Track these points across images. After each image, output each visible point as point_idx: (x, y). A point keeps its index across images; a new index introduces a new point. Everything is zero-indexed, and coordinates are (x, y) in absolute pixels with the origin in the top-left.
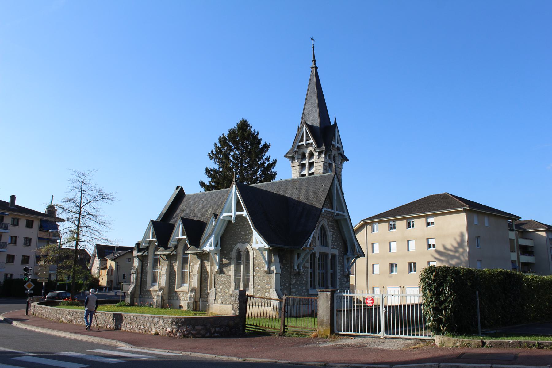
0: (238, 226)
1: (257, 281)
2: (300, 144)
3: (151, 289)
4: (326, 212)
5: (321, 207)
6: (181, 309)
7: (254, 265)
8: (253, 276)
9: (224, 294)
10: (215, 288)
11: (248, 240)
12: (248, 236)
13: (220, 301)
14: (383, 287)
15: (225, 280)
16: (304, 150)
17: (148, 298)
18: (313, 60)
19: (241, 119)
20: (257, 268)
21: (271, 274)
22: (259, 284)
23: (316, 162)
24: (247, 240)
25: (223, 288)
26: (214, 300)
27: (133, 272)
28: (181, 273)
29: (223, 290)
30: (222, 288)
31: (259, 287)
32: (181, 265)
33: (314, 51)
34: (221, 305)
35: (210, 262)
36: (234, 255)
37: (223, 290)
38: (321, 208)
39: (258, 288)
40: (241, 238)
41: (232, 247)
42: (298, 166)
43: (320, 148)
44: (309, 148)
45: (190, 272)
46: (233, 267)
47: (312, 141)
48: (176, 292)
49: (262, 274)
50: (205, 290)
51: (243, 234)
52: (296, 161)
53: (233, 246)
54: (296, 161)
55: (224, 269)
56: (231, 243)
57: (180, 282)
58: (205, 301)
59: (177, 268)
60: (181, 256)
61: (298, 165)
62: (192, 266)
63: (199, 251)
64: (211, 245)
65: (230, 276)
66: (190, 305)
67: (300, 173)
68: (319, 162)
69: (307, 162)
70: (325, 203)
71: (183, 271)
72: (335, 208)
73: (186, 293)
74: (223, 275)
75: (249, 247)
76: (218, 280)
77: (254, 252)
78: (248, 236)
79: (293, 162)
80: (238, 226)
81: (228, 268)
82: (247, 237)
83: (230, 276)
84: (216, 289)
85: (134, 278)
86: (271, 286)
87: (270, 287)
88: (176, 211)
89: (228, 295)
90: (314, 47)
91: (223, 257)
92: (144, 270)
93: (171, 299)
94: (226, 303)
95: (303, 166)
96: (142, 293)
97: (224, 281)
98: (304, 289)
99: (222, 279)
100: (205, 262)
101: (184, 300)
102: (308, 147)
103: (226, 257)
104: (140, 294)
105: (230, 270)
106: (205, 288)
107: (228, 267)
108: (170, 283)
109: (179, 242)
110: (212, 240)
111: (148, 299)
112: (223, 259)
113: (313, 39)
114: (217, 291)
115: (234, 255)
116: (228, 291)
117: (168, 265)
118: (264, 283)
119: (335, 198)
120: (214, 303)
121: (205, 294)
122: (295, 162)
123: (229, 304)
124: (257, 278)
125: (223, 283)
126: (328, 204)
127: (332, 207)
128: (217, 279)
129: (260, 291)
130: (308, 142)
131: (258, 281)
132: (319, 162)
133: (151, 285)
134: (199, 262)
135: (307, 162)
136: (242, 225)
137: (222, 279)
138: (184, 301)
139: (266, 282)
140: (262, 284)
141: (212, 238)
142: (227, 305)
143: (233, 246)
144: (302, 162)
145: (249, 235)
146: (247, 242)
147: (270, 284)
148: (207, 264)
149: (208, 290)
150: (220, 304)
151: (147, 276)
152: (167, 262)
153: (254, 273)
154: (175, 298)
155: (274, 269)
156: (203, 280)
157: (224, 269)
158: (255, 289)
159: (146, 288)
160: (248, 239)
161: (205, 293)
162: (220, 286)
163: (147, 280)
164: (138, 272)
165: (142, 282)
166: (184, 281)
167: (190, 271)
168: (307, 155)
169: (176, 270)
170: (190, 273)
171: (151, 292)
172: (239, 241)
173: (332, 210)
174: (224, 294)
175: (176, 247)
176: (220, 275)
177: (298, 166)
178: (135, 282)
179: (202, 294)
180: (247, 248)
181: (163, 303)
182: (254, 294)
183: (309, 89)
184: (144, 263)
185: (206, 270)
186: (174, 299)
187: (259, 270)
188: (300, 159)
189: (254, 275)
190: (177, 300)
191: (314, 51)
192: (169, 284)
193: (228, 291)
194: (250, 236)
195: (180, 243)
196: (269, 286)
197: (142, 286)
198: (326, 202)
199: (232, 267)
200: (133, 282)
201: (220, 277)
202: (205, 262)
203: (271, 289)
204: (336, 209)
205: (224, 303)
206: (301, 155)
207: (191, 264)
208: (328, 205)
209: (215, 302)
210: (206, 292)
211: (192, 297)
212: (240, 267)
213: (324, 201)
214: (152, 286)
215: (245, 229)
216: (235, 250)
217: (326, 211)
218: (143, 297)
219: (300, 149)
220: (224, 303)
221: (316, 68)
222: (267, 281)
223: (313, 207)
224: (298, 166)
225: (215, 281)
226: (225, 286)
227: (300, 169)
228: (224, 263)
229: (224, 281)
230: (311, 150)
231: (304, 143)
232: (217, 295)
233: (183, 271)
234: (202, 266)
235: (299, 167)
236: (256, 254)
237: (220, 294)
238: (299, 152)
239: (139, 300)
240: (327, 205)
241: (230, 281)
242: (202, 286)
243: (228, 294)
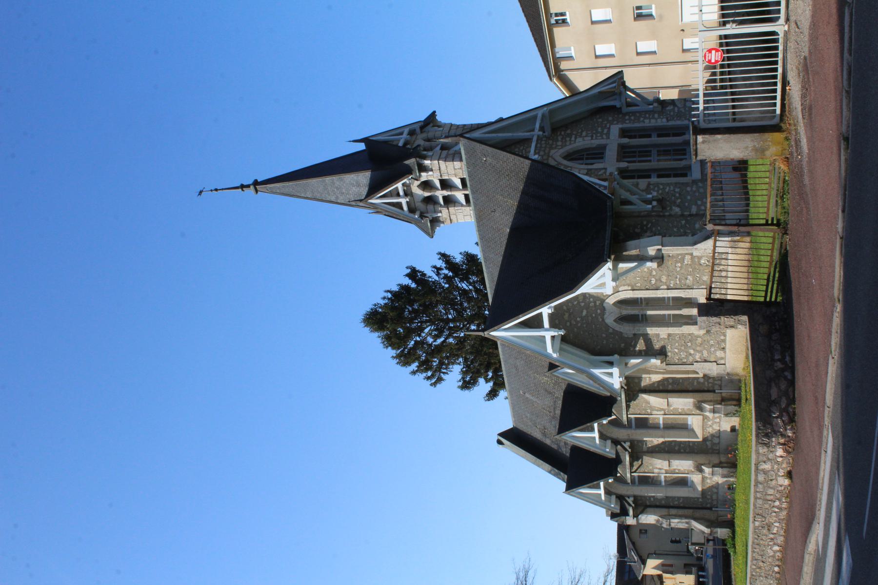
0: (571, 323)
1: (678, 282)
2: (405, 208)
3: (700, 489)
4: (537, 151)
5: (528, 162)
6: (737, 428)
7: (647, 289)
8: (668, 289)
9: (706, 346)
10: (695, 364)
11: (598, 303)
12: (591, 302)
13: (720, 354)
14: (682, 32)
15: (677, 344)
16: (418, 200)
17: (717, 493)
18: (240, 190)
19: (363, 325)
20: (653, 282)
21: (663, 254)
22: (684, 278)
23: (441, 176)
24: (598, 304)
25: (694, 347)
26: (718, 364)
27: (668, 523)
28: (667, 432)
29: (698, 348)
30: (694, 350)
31: (689, 277)
32: (651, 431)
33: (222, 189)
34: (727, 351)
35: (644, 376)
36: (627, 329)
37: (698, 348)
38: (530, 162)
39: (691, 279)
40: (594, 315)
41: (611, 334)
42: (448, 209)
43: (413, 168)
44: (413, 191)
45: (665, 412)
46: (652, 330)
47: (399, 185)
48: (705, 439)
49: (665, 272)
50: (699, 383)
51: (587, 312)
52: (439, 215)
53: (611, 331)
54: (439, 215)
55: (657, 346)
56: (604, 335)
57: (684, 432)
58: (720, 382)
59: (657, 439)
60: (633, 431)
61: (447, 210)
62: (653, 410)
63: (623, 396)
64: (611, 374)
65: (669, 335)
66: (729, 411)
67: (462, 205)
68: (440, 170)
69: (440, 194)
70: (520, 154)
71: (662, 426)
72: (528, 134)
73: (706, 420)
74: (669, 348)
75: (611, 301)
76: (677, 358)
77: (620, 289)
78: (591, 302)
79: (442, 220)
80: (571, 323)
81: (654, 340)
82: (592, 304)
83: (669, 335)
84: (697, 362)
85: (678, 522)
86: (687, 254)
87: (690, 257)
89: (707, 337)
90: (216, 190)
91: (632, 349)
92: (663, 502)
93: (718, 448)
94: (723, 342)
95: (449, 201)
96: (708, 506)
97: (679, 347)
99: (676, 350)
100: (643, 384)
101: (719, 423)
102: (411, 192)
103: (633, 344)
104: (710, 509)
105: (658, 335)
106: (695, 384)
107: (652, 339)
108: (687, 451)
109: (607, 436)
110: (601, 373)
112: (637, 349)
113: (201, 192)
114: (699, 360)
115: (627, 329)
116: (699, 339)
117: (653, 457)
118: (681, 267)
119: (510, 134)
120: (724, 364)
121: (706, 383)
122: (442, 216)
123: (725, 336)
124: (672, 282)
125: (683, 348)
126: (521, 148)
127: (528, 141)
128: (677, 360)
129: (698, 275)
130: (401, 193)
131: (677, 279)
132: (440, 170)
133: (692, 489)
134: (645, 396)
135: (440, 194)
136: (570, 315)
137: (676, 350)
138: (721, 423)
140: (683, 271)
141: (597, 372)
142: (728, 338)
143: (611, 331)
145: (588, 300)
146: (603, 305)
147: (683, 256)
148: (648, 381)
149: (698, 378)
150: (725, 352)
151: (675, 497)
152: (646, 459)
153: (662, 287)
154: (716, 441)
155: (654, 250)
156: (679, 388)
157: (657, 346)
158: (693, 285)
159: (698, 498)
160: (595, 302)
161: (703, 383)
162: (690, 354)
163: (683, 498)
164: (668, 515)
165: (687, 506)
166: (682, 424)
167: (662, 412)
168: (427, 194)
169: (661, 440)
170: (667, 413)
171: (705, 488)
172: (601, 320)
173: (532, 139)
174: (706, 346)
175: (616, 442)
176: (669, 354)
177: (450, 210)
178: (687, 520)
179: (706, 389)
180: (613, 304)
181: (726, 465)
182: (705, 287)
183: (298, 194)
184: (648, 503)
185: (659, 382)
186: (719, 443)
187: (657, 278)
188: (435, 206)
189: (665, 287)
190: (719, 437)
191: (222, 189)
192: (688, 453)
193: (700, 337)
194: (589, 299)
195: (609, 435)
196: (688, 257)
197: (694, 506)
198: (517, 153)
199: (651, 331)
200: (687, 523)
201: (673, 355)
202: (643, 384)
203: (692, 253)
204: (532, 133)
205: (723, 345)
206: (427, 206)
207: (649, 411)
208: (523, 149)
209: (722, 362)
210: (702, 380)
211: (712, 407)
212: (651, 315)
213: (515, 157)
214: (693, 486)
215: (577, 308)
216: (618, 327)
217: (535, 151)
218: (715, 503)
219: (416, 208)
220: (723, 345)
221: (256, 183)
222: (677, 262)
223: (528, 178)
224: (448, 209)
225: (680, 363)
226: (689, 344)
227: (455, 207)
228: (644, 348)
229: (679, 347)
230: (418, 186)
231: (404, 201)
232: (708, 359)
233: (662, 426)
234: (653, 390)
236: (624, 285)
238: (422, 210)
239: (721, 511)
240: (524, 151)
241: (678, 334)
242: (691, 389)
243: (706, 339)
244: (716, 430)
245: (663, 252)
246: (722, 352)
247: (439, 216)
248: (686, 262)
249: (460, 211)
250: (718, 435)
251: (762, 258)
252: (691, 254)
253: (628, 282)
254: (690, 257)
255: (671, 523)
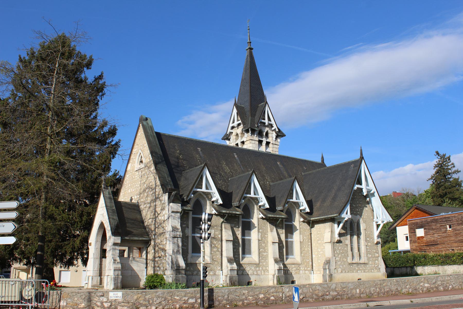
1: (368, 250)
12: (358, 209)
13: (340, 270)
14: (76, 271)
16: (263, 128)
17: (192, 275)
23: (273, 144)
25: (342, 257)
34: (342, 274)
40: (353, 210)
45: (260, 240)
52: (255, 136)
54: (255, 136)
65: (347, 245)
66: (281, 279)
68: (276, 144)
74: (341, 244)
83: (347, 245)
86: (379, 255)
88: (167, 153)
95: (260, 142)
98: (44, 272)
99: (340, 248)
111: (194, 277)
123: (348, 272)
137: (340, 248)
139: (375, 251)
144: (260, 139)
147: (378, 253)
150: (340, 273)
160: (359, 211)
162: (338, 255)
176: (338, 244)
178: (181, 251)
193: (347, 260)
199: (349, 237)
205: (343, 272)
207: (260, 231)
221: (251, 49)
226: (343, 255)
235: (257, 142)
237: (339, 263)
244: (248, 272)
245: (379, 245)
246: (341, 271)
247: (254, 135)
248: (376, 254)
249: (256, 146)
250: (244, 274)
251: (206, 305)
252: (379, 256)
253: (367, 228)
254: (378, 256)
255: (176, 239)
